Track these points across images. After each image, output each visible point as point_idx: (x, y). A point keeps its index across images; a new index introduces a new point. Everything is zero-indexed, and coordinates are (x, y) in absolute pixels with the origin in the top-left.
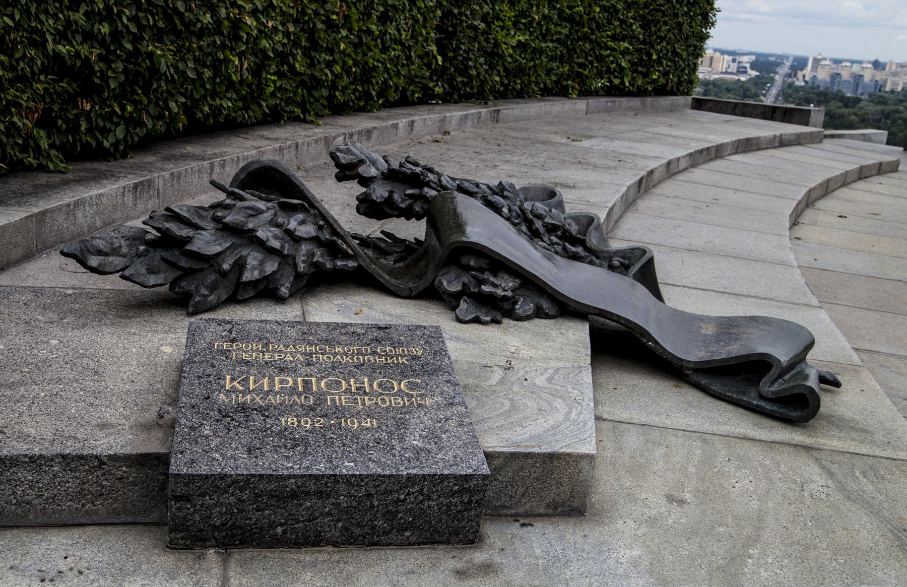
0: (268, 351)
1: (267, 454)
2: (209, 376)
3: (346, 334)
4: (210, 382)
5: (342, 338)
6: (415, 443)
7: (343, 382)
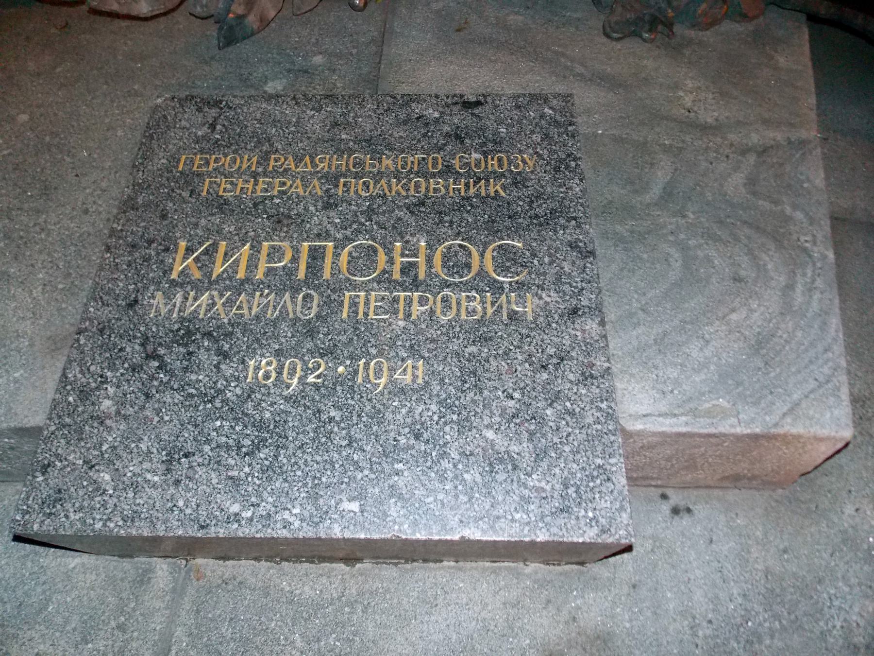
0: (265, 174)
1: (201, 471)
2: (150, 242)
3: (405, 122)
4: (147, 259)
7: (381, 250)
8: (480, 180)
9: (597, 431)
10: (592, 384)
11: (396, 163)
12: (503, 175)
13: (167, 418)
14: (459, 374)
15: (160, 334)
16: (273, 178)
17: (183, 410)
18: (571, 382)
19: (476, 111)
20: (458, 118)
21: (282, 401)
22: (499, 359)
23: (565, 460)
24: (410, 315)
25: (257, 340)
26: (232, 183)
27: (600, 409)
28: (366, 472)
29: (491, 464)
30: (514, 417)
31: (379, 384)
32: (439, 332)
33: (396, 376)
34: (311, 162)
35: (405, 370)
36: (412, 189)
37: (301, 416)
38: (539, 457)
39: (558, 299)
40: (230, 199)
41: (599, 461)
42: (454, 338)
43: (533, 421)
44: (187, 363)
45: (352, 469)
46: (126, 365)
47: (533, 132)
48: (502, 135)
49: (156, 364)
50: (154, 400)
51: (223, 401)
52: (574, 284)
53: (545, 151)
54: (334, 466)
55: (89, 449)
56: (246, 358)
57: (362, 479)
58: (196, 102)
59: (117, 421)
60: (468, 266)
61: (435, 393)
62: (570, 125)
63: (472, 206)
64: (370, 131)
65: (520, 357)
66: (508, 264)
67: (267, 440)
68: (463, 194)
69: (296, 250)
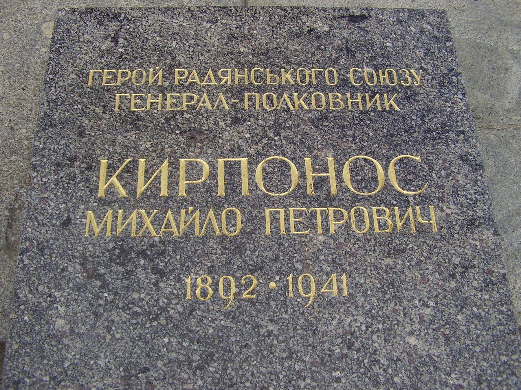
0: (172, 89)
2: (72, 160)
3: (298, 35)
4: (73, 178)
5: (293, 46)
6: (412, 340)
8: (376, 94)
9: (500, 332)
10: (493, 290)
11: (294, 77)
12: (394, 90)
13: (118, 336)
14: (379, 286)
15: (97, 253)
16: (179, 93)
17: (131, 328)
18: (476, 289)
19: (362, 25)
20: (346, 32)
21: (222, 317)
22: (413, 270)
23: (477, 359)
24: (328, 230)
25: (189, 257)
26: (141, 98)
27: (501, 312)
28: (308, 381)
29: (415, 368)
30: (431, 323)
31: (309, 298)
32: (357, 246)
33: (323, 290)
34: (215, 76)
35: (330, 283)
36: (313, 102)
37: (240, 330)
38: (455, 357)
39: (457, 211)
40: (142, 115)
41: (504, 358)
42: (371, 251)
43: (448, 326)
44: (127, 282)
45: (295, 378)
46: (71, 285)
47: (416, 47)
48: (389, 49)
49: (99, 284)
50: (103, 319)
51: (167, 319)
52: (469, 196)
53: (429, 66)
54: (278, 377)
55: (52, 366)
56: (182, 276)
57: (305, 387)
58: (96, 15)
59: (72, 340)
60: (375, 179)
61: (360, 304)
62: (447, 41)
63: (371, 120)
64: (267, 44)
65: (431, 268)
66: (410, 178)
67: (214, 355)
68: (361, 108)
69: (213, 167)
